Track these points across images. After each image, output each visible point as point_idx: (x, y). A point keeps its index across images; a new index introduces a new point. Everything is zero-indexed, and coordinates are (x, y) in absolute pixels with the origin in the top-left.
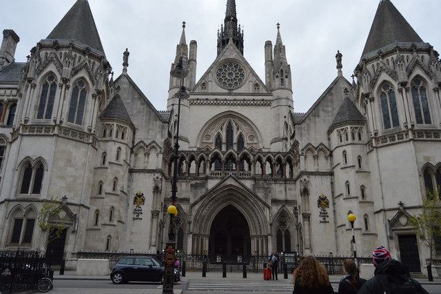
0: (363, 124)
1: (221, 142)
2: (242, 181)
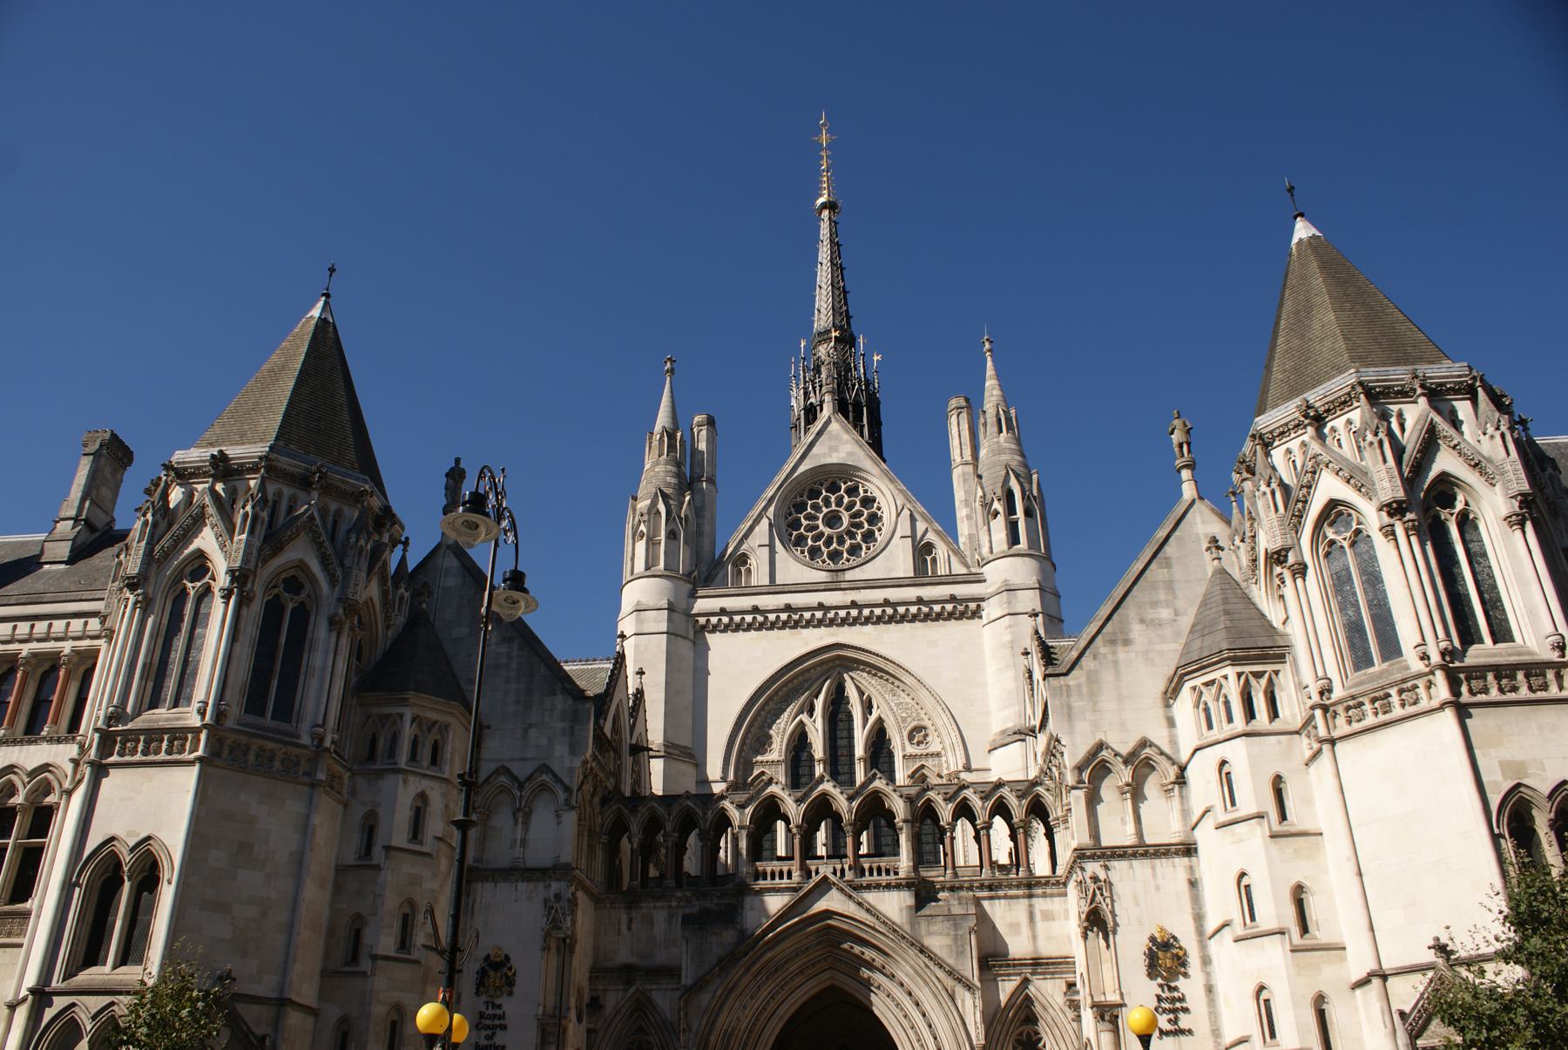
0: (1280, 658)
1: (811, 757)
2: (870, 897)
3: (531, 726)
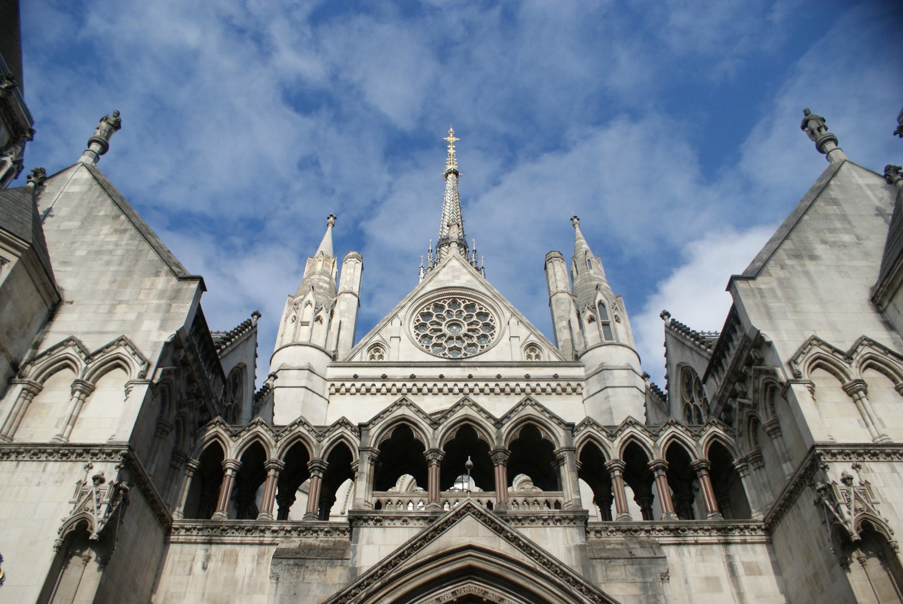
3: (120, 302)
